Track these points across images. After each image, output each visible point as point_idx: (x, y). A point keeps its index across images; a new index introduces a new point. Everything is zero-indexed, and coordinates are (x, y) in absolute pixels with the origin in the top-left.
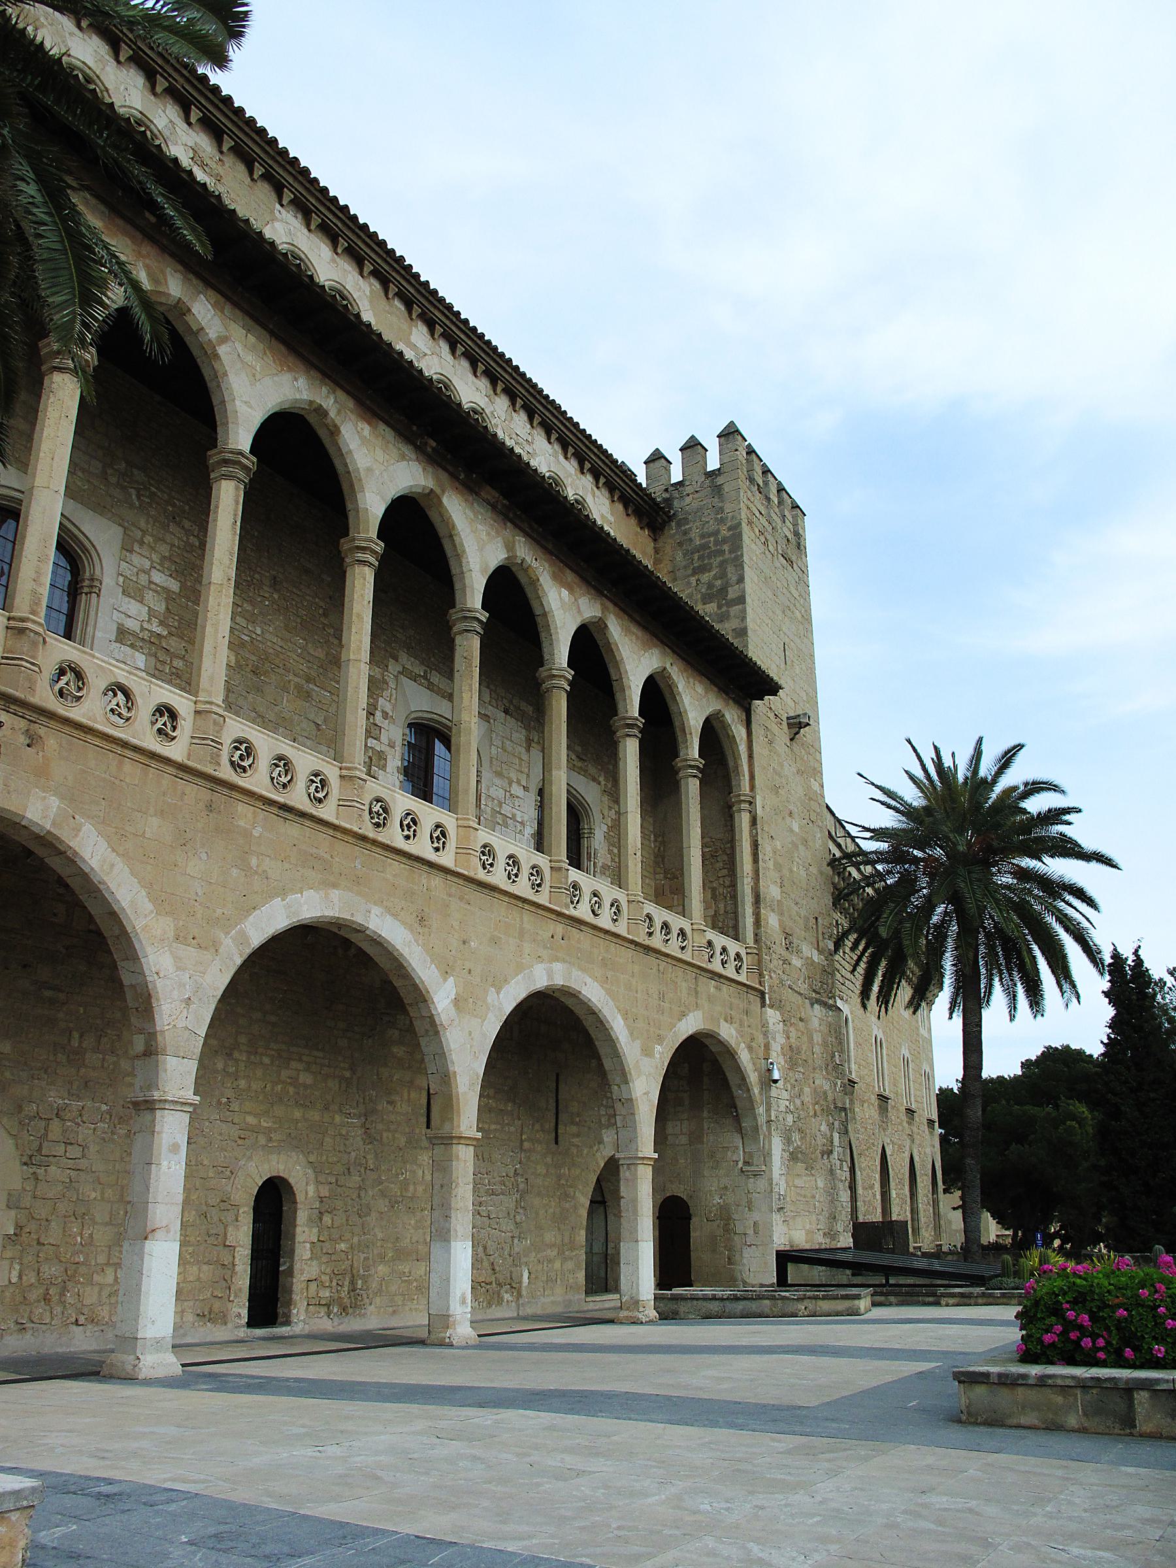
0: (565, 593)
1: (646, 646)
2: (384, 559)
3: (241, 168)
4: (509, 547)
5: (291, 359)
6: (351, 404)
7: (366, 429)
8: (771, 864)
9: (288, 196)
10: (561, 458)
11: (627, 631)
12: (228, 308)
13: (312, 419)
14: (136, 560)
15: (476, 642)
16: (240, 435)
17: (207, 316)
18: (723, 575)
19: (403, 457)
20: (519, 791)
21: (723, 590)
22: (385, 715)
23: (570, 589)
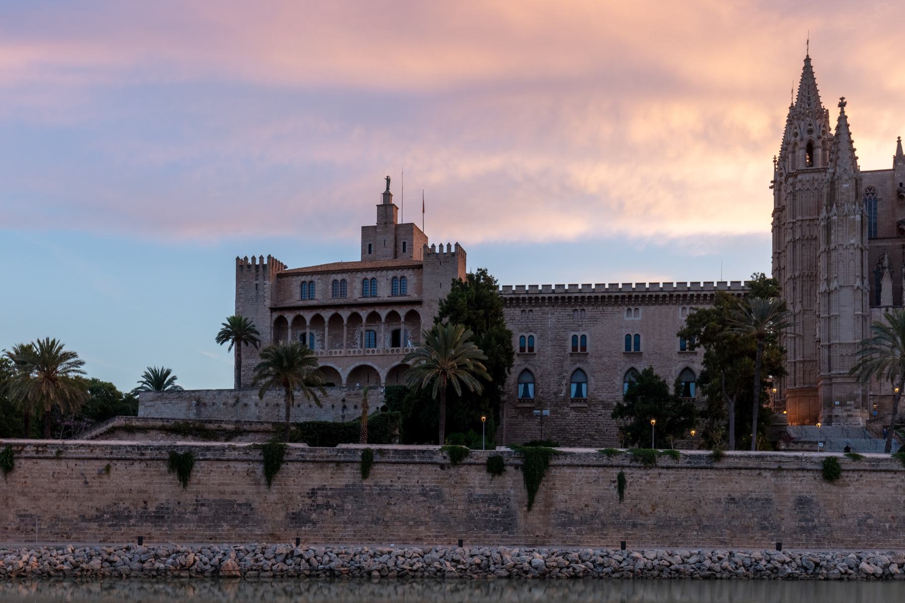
17: (302, 313)
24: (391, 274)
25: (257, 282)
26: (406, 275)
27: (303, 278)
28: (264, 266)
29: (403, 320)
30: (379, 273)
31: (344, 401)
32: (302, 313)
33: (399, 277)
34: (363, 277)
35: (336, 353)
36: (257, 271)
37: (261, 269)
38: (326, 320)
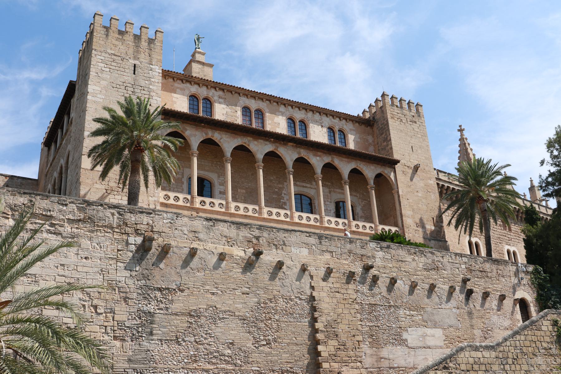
0: (318, 158)
1: (349, 162)
2: (264, 167)
3: (230, 94)
4: (299, 153)
5: (236, 136)
6: (251, 139)
7: (256, 142)
8: (407, 206)
9: (241, 94)
10: (333, 120)
11: (342, 161)
12: (221, 133)
13: (244, 144)
14: (221, 178)
15: (291, 176)
16: (228, 154)
17: (217, 136)
18: (386, 134)
19: (266, 144)
20: (329, 203)
21: (387, 138)
22: (285, 194)
23: (320, 156)
24: (327, 121)
25: (137, 62)
26: (345, 127)
27: (194, 89)
28: (151, 41)
29: (372, 182)
30: (310, 114)
31: (465, 281)
32: (217, 136)
33: (336, 129)
34: (288, 114)
35: (278, 214)
36: (137, 46)
37: (144, 44)
38: (260, 156)
